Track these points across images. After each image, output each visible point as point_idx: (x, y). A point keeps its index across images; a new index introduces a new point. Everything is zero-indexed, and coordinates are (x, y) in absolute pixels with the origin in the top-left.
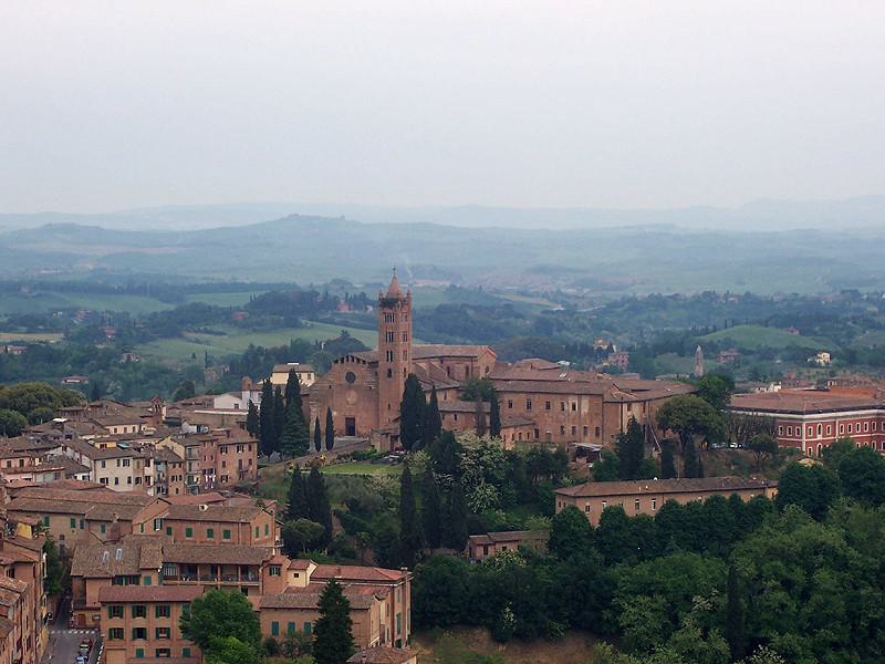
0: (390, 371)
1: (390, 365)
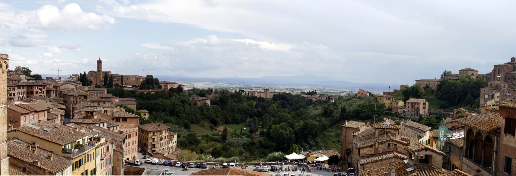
0: (99, 74)
1: (99, 72)
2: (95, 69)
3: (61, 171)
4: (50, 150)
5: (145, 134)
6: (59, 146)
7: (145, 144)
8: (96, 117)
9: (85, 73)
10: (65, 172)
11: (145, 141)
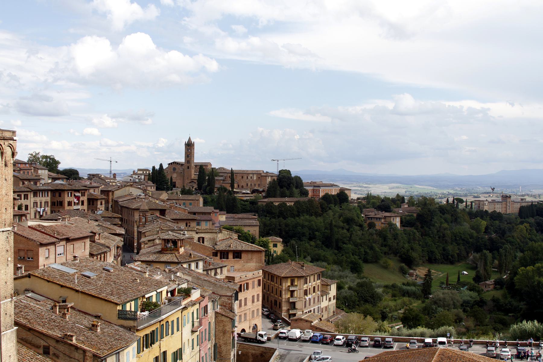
1: (188, 165)
2: (181, 159)
3: (116, 354)
4: (94, 314)
5: (276, 283)
6: (112, 305)
7: (276, 301)
8: (182, 250)
9: (161, 165)
10: (124, 356)
11: (276, 296)
